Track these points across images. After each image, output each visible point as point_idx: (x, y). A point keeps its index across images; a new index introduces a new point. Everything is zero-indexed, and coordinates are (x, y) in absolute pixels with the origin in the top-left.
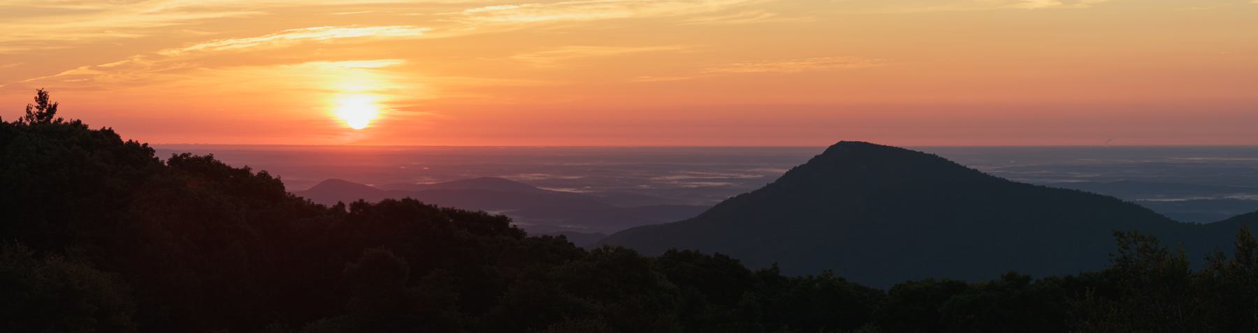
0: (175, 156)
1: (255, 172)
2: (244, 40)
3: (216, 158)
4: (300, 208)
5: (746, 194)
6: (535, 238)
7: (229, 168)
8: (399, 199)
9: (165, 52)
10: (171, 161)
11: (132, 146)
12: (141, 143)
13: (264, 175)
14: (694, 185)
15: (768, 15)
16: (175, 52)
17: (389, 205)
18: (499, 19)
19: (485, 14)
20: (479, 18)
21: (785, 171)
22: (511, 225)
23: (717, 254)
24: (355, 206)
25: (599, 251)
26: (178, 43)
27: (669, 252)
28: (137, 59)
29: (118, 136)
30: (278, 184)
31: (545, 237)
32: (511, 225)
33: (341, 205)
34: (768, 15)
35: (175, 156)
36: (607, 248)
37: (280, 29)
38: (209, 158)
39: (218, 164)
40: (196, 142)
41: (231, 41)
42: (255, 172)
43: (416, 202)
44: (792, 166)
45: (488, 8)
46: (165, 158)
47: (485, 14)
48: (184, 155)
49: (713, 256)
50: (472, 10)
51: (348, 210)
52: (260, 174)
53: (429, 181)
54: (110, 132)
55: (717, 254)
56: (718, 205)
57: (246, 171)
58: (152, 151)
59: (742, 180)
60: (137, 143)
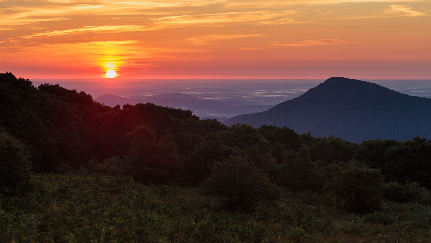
0: (42, 85)
1: (79, 92)
2: (60, 32)
3: (61, 85)
4: (105, 109)
5: (290, 100)
6: (204, 120)
7: (67, 90)
8: (145, 103)
9: (25, 37)
10: (39, 87)
11: (21, 81)
12: (26, 79)
13: (83, 93)
14: (266, 96)
15: (292, 20)
16: (29, 37)
17: (140, 106)
18: (173, 22)
19: (167, 20)
20: (163, 22)
21: (306, 90)
22: (193, 114)
23: (284, 127)
24: (125, 106)
25: (235, 126)
26: (30, 32)
27: (263, 126)
28: (11, 40)
29: (14, 76)
30: (89, 97)
31: (208, 120)
32: (193, 114)
33: (118, 106)
34: (292, 20)
35: (42, 85)
36: (238, 125)
37: (78, 27)
38: (57, 85)
39: (62, 88)
40: (51, 79)
41: (55, 32)
42: (79, 92)
43: (152, 104)
44: (310, 88)
45: (168, 17)
46: (36, 85)
47: (167, 20)
48: (46, 84)
49: (282, 128)
50: (161, 19)
51: (122, 108)
52: (81, 93)
53: (149, 95)
54: (10, 74)
55: (284, 127)
56: (277, 105)
57: (75, 91)
58: (31, 83)
59: (287, 94)
60: (24, 79)
